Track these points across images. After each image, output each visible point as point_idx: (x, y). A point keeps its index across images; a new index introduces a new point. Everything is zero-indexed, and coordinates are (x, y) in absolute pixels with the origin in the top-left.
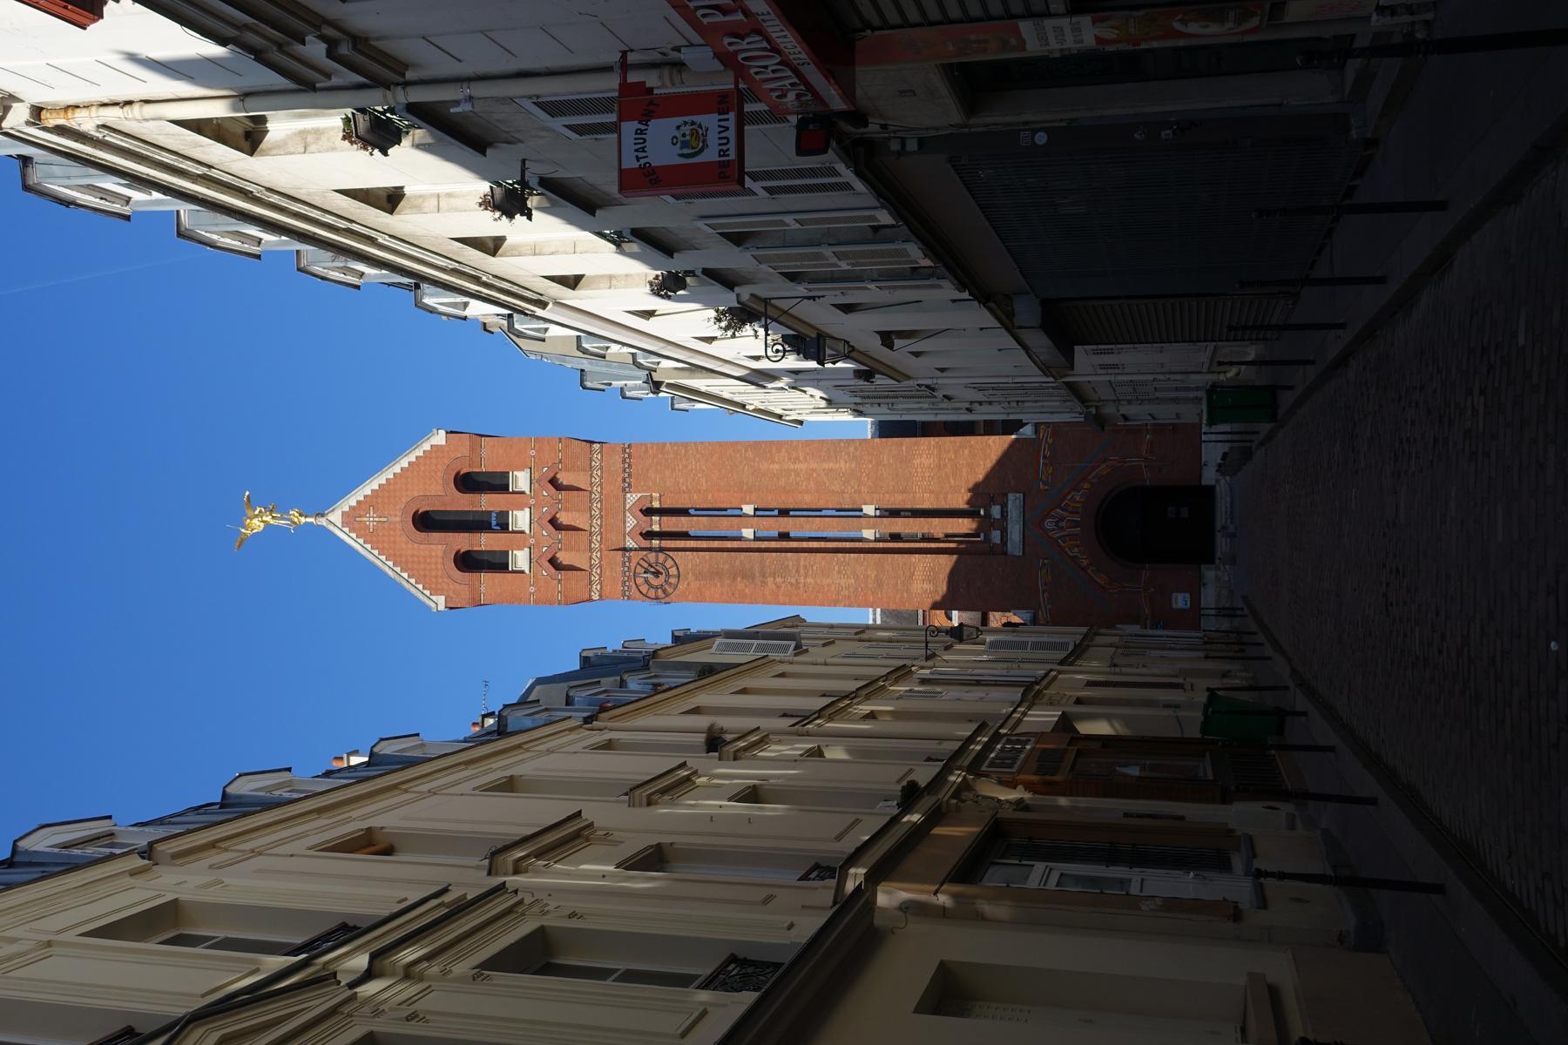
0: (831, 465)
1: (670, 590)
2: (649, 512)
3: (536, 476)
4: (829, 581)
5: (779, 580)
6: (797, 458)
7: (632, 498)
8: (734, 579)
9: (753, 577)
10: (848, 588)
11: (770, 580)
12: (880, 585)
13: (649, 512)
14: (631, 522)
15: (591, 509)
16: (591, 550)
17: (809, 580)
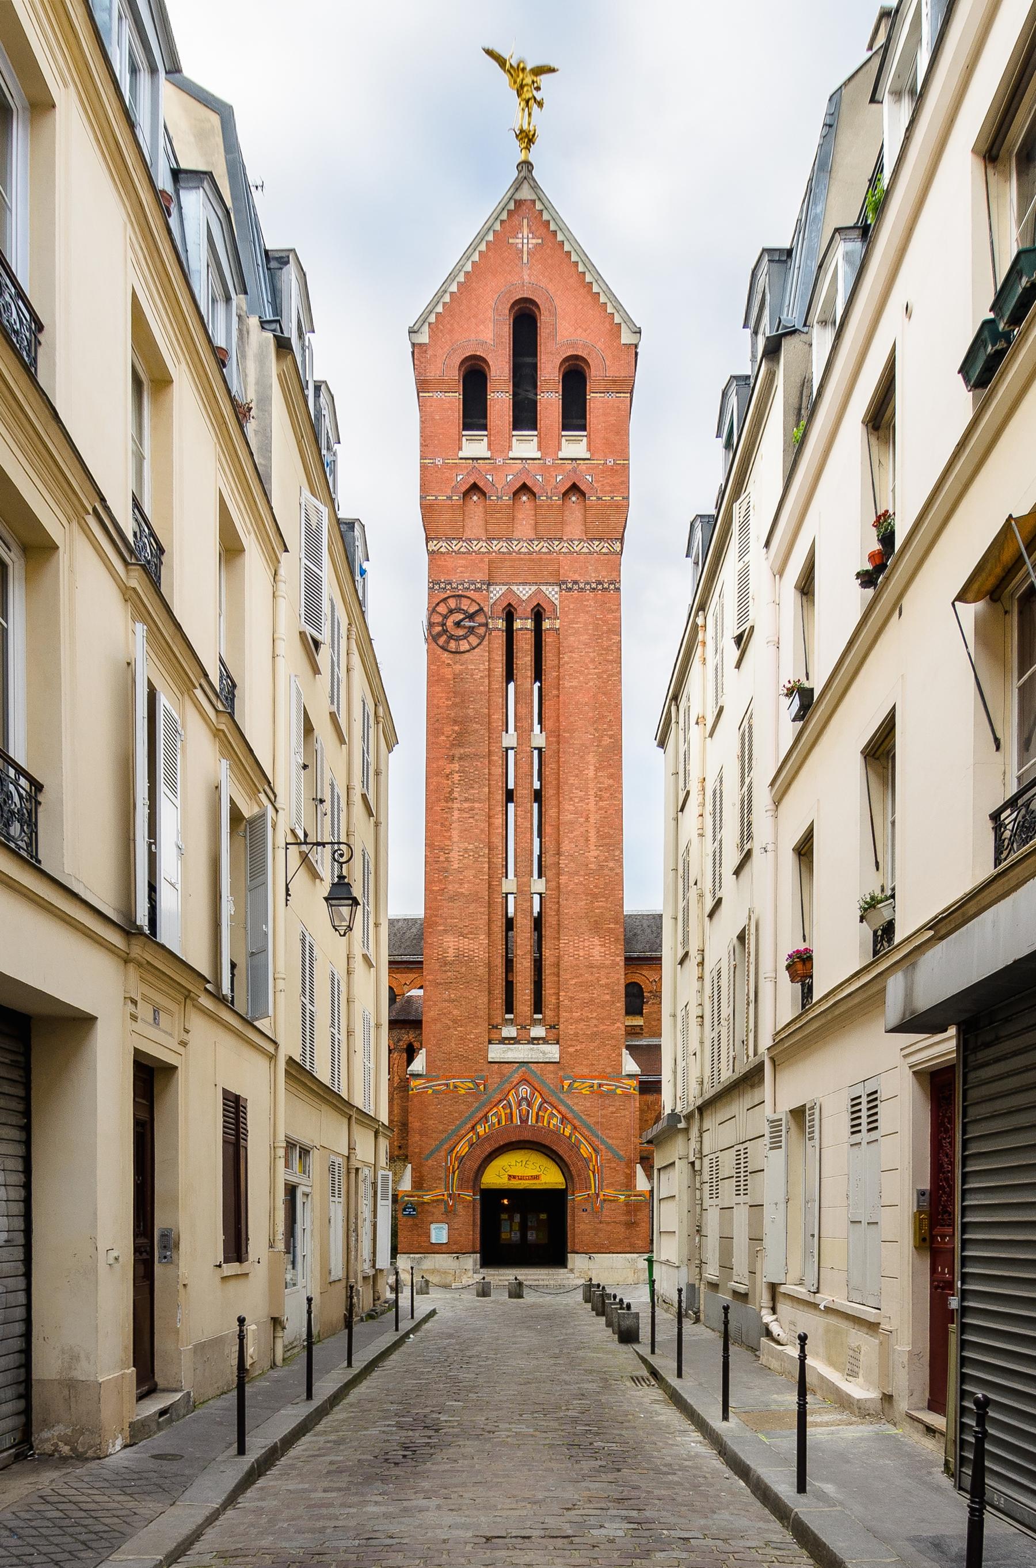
0: (593, 839)
1: (442, 640)
2: (538, 616)
3: (583, 466)
4: (456, 839)
5: (456, 777)
6: (601, 799)
7: (552, 593)
8: (455, 722)
9: (460, 745)
10: (447, 860)
11: (456, 766)
12: (452, 899)
13: (538, 616)
14: (524, 592)
15: (540, 539)
16: (490, 539)
17: (456, 813)
